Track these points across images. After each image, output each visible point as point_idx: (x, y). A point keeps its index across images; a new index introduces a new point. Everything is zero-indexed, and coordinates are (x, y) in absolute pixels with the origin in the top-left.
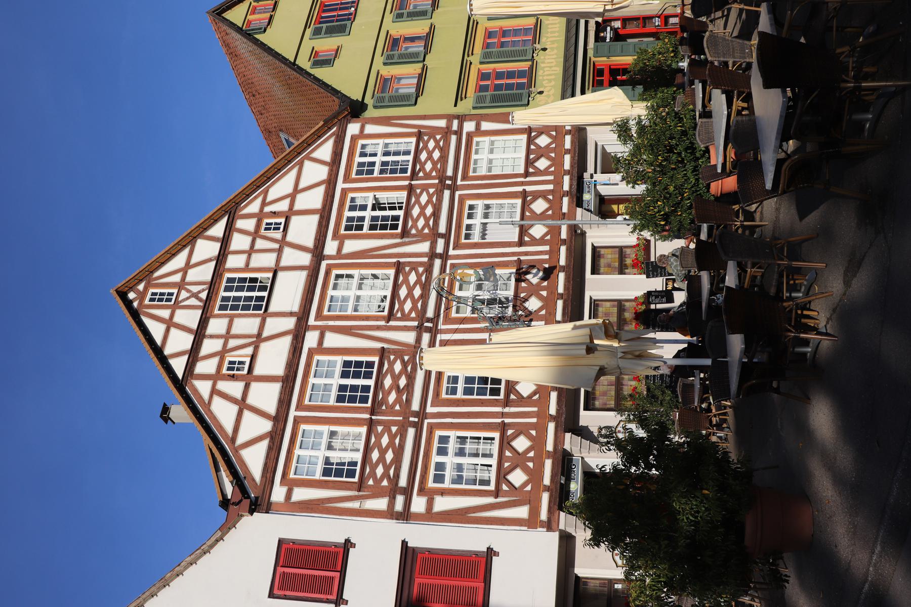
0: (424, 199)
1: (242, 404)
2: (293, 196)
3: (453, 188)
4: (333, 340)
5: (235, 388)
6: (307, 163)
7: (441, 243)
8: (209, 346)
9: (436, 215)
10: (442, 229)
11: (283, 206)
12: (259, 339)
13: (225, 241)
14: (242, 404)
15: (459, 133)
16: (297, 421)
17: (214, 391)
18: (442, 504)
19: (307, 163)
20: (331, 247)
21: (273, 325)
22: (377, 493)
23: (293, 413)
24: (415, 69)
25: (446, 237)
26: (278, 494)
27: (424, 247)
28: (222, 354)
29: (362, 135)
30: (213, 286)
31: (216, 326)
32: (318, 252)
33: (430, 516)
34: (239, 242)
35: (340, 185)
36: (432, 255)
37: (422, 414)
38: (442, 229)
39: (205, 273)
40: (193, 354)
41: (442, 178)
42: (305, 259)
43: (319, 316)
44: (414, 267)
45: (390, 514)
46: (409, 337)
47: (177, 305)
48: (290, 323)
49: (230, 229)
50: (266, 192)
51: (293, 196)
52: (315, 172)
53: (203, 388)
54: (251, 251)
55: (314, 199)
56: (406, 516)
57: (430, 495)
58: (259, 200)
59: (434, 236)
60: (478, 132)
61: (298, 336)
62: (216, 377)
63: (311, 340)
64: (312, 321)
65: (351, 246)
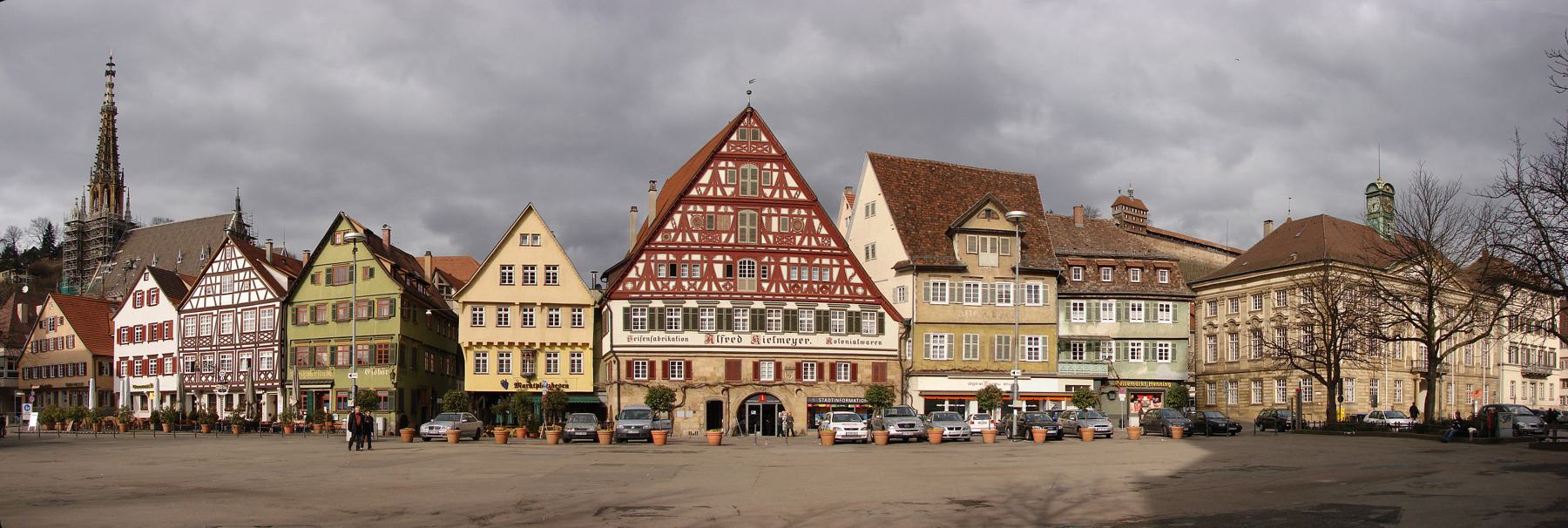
0: (251, 338)
3: (256, 347)
6: (265, 291)
7: (239, 347)
9: (247, 343)
10: (243, 346)
15: (274, 345)
16: (196, 315)
19: (265, 291)
20: (239, 309)
24: (309, 321)
25: (241, 348)
26: (182, 316)
27: (237, 342)
35: (258, 306)
36: (235, 345)
37: (199, 351)
38: (243, 346)
40: (213, 274)
43: (221, 312)
44: (232, 340)
45: (179, 348)
46: (214, 344)
48: (218, 304)
50: (258, 278)
55: (254, 298)
58: (255, 277)
59: (240, 344)
63: (215, 312)
64: (220, 310)
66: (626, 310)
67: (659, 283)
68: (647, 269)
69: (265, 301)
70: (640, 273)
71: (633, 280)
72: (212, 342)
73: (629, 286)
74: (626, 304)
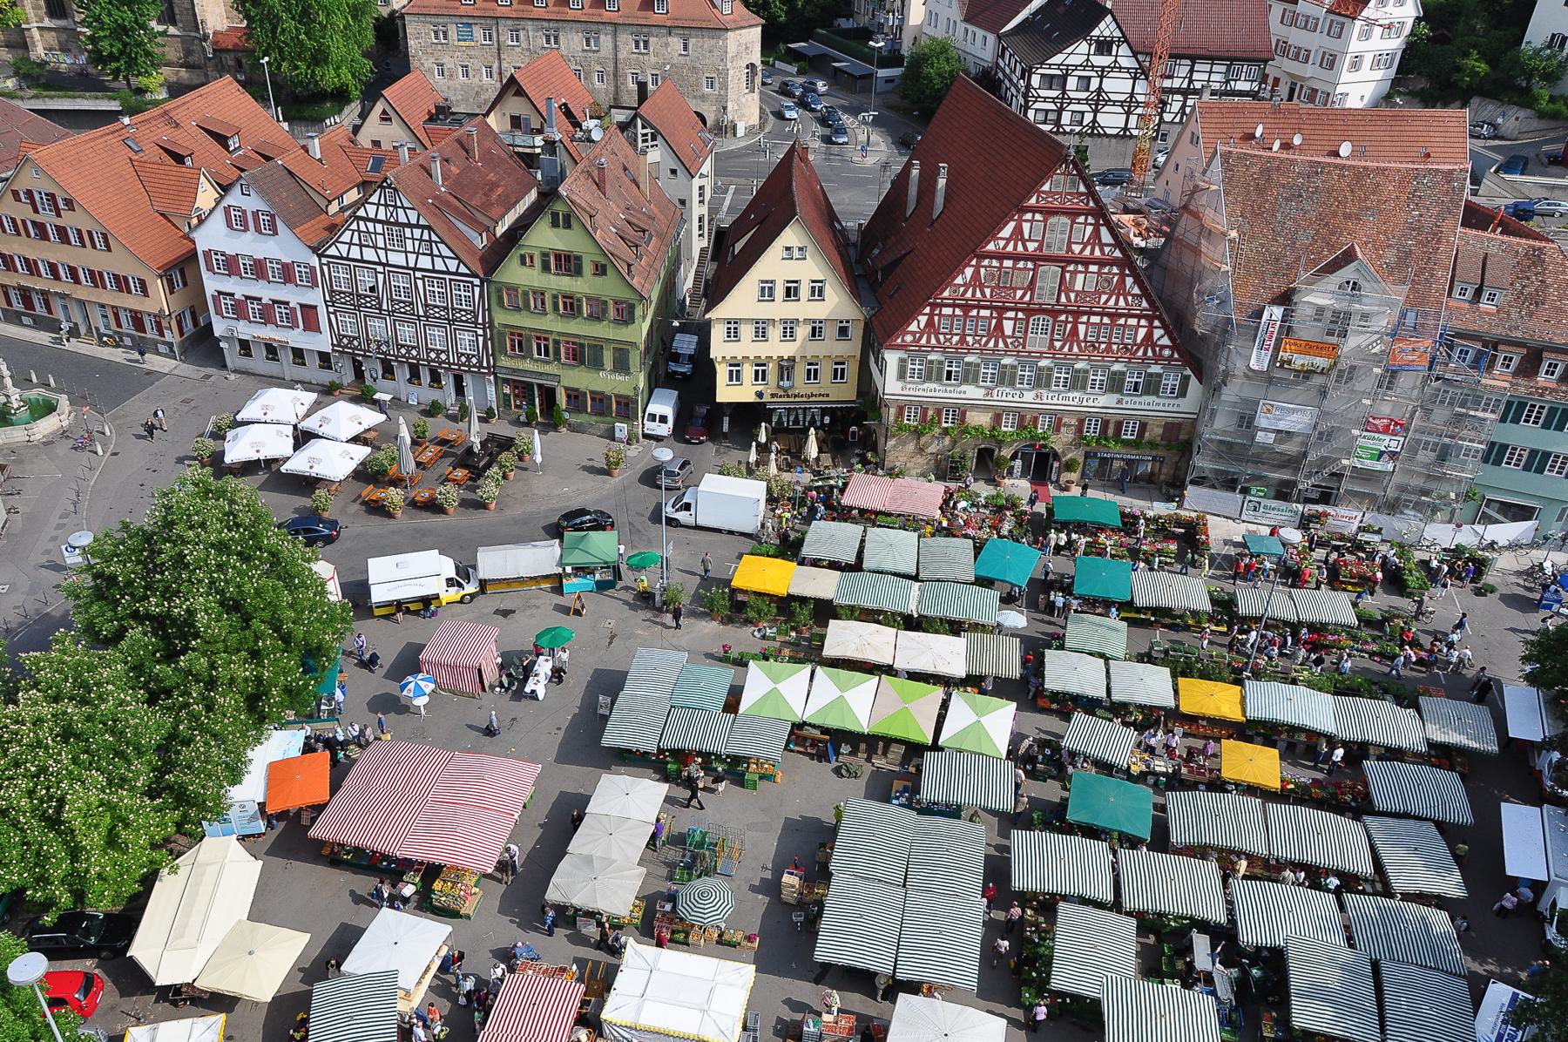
1: (350, 244)
2: (441, 256)
4: (381, 277)
5: (356, 240)
8: (370, 225)
11: (436, 252)
12: (375, 247)
13: (417, 226)
14: (350, 244)
17: (354, 231)
18: (332, 316)
20: (418, 274)
21: (382, 253)
22: (331, 296)
23: (352, 263)
27: (421, 313)
28: (368, 232)
29: (473, 285)
30: (397, 224)
31: (379, 227)
32: (415, 269)
33: (328, 313)
34: (417, 233)
36: (419, 316)
39: (402, 219)
40: (366, 219)
41: (454, 320)
42: (412, 264)
46: (385, 307)
47: (386, 205)
49: (423, 227)
51: (441, 256)
52: (453, 265)
53: (354, 226)
54: (413, 239)
55: (439, 265)
56: (327, 306)
57: (335, 313)
60: (477, 335)
61: (380, 263)
62: (359, 231)
63: (380, 269)
65: (420, 283)
66: (902, 361)
67: (941, 337)
68: (930, 323)
69: (456, 273)
70: (922, 326)
71: (913, 333)
72: (380, 304)
73: (909, 338)
74: (901, 354)
